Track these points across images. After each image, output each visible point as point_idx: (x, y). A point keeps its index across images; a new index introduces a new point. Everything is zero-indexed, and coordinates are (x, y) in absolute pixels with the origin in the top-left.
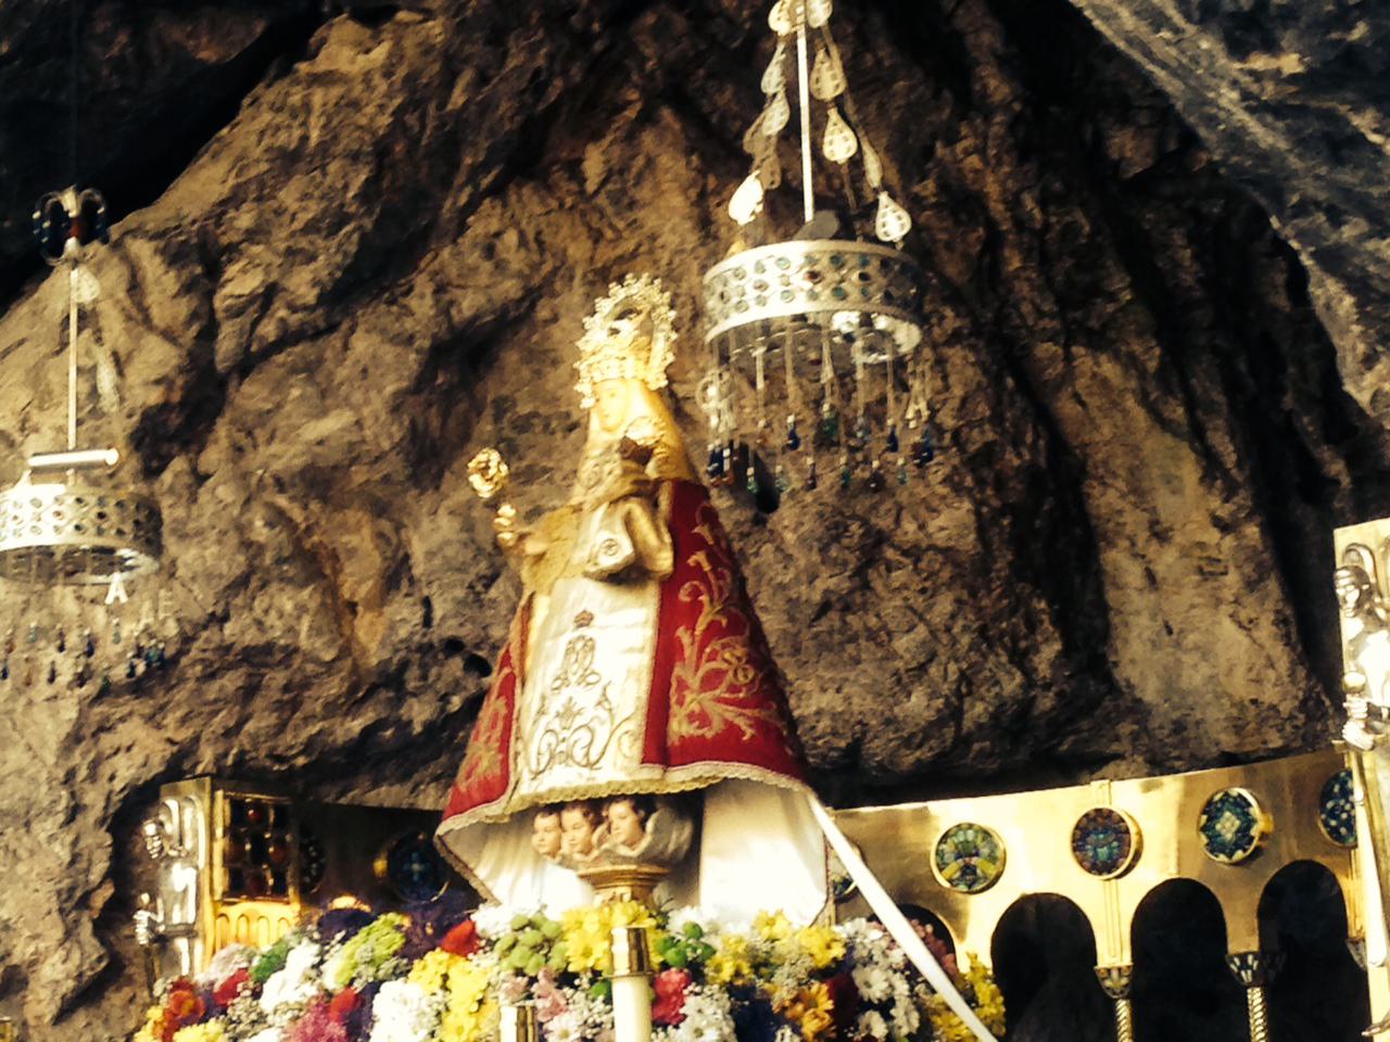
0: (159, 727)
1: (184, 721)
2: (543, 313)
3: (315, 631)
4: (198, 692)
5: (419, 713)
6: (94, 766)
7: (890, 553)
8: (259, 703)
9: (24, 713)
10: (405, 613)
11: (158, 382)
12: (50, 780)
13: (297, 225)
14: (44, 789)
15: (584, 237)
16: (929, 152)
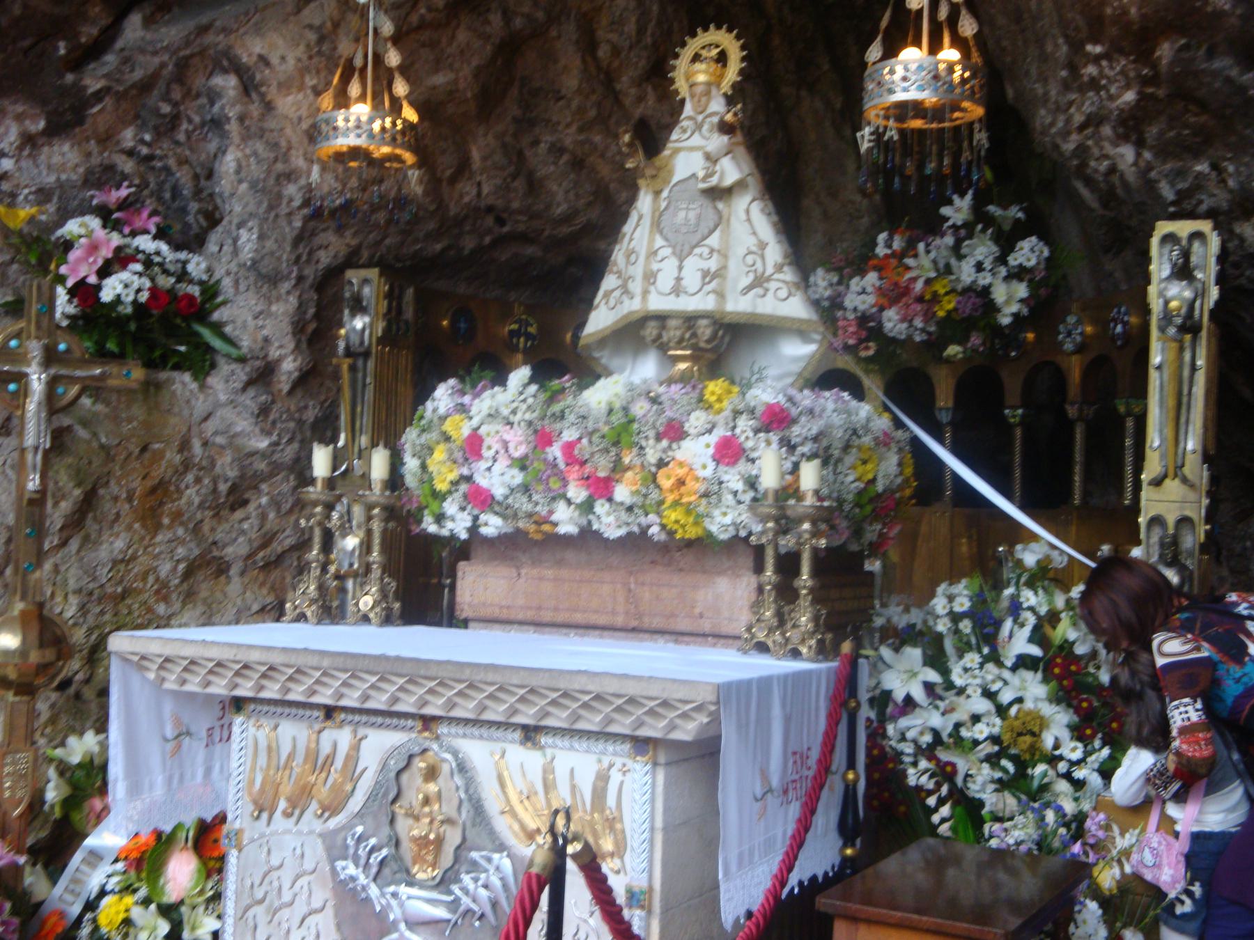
0: (342, 236)
2: (554, 33)
5: (469, 243)
6: (310, 254)
10: (468, 189)
12: (288, 261)
14: (284, 265)
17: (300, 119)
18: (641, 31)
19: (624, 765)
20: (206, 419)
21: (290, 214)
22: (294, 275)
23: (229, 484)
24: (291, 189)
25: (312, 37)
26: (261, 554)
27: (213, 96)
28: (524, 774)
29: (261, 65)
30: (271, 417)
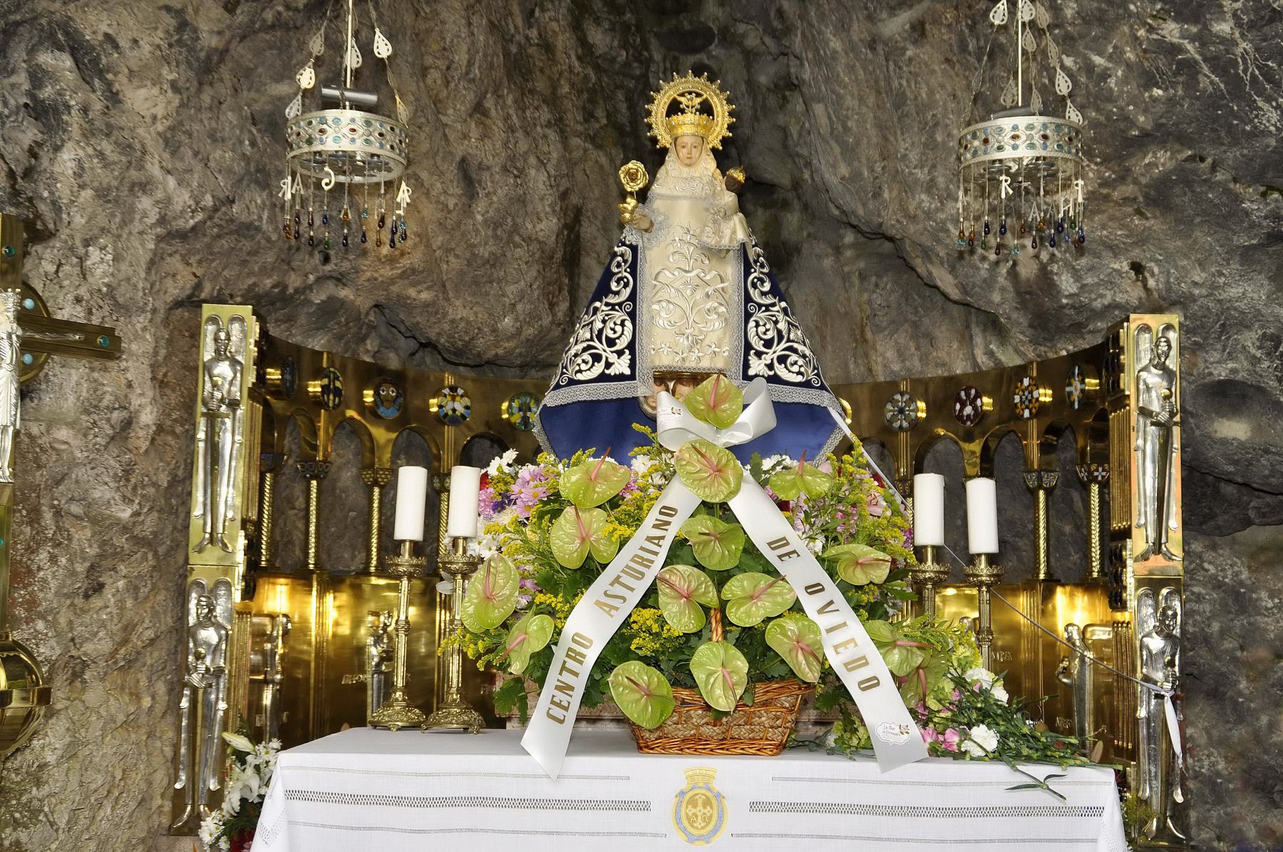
0: (188, 264)
1: (200, 262)
4: (209, 246)
5: (294, 281)
7: (517, 239)
9: (128, 239)
11: (220, 33)
12: (144, 289)
14: (141, 294)
15: (411, 11)
16: (532, 13)
17: (154, 118)
18: (470, 63)
20: (58, 483)
21: (141, 233)
23: (87, 564)
24: (145, 203)
25: (170, 21)
26: (122, 651)
27: (38, 77)
29: (108, 47)
30: (133, 480)
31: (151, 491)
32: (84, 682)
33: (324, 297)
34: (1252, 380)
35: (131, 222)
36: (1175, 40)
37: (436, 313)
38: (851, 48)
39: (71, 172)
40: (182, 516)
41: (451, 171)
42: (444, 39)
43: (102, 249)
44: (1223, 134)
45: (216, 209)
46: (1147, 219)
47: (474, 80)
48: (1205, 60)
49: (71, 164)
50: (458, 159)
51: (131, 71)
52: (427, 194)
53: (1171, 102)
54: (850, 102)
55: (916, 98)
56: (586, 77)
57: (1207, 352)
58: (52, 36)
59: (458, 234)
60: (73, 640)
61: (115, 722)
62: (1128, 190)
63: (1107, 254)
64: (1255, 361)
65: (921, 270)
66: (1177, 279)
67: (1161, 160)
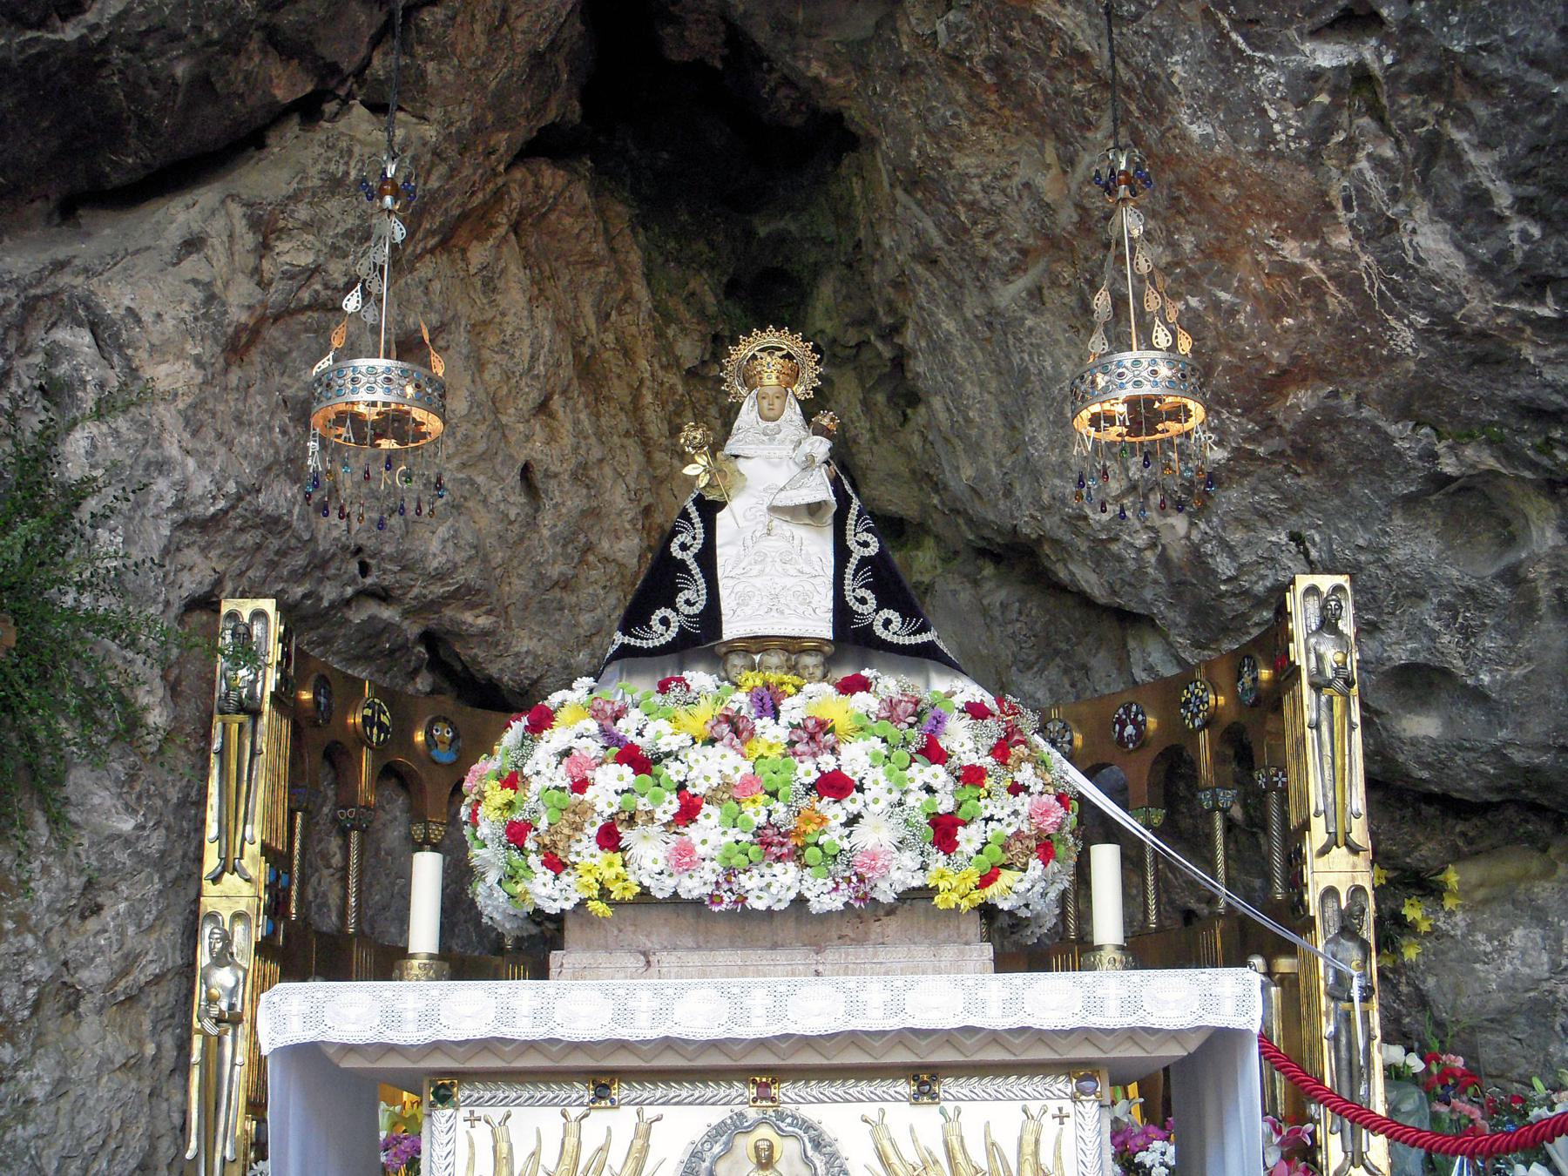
1: (221, 556)
3: (302, 517)
4: (231, 541)
5: (329, 593)
8: (259, 558)
11: (250, 307)
13: (339, 230)
16: (608, 315)
18: (533, 358)
19: (1060, 1110)
22: (162, 598)
24: (161, 485)
25: (198, 295)
26: (122, 984)
27: (53, 355)
28: (915, 1141)
29: (129, 320)
30: (138, 789)
31: (159, 803)
32: (78, 1016)
33: (364, 616)
34: (1434, 662)
35: (145, 504)
36: (1297, 261)
37: (497, 644)
38: (968, 327)
39: (82, 451)
40: (194, 844)
41: (513, 478)
42: (503, 331)
43: (112, 530)
44: (1361, 362)
45: (240, 498)
46: (1298, 475)
47: (538, 376)
48: (1330, 278)
49: (85, 443)
50: (520, 465)
51: (152, 346)
52: (485, 501)
53: (1303, 330)
54: (969, 389)
55: (1040, 373)
56: (672, 388)
57: (1382, 631)
58: (73, 310)
59: (521, 549)
60: (65, 964)
61: (112, 1063)
62: (1276, 443)
63: (1262, 525)
64: (1433, 635)
65: (1063, 574)
66: (1340, 545)
67: (1303, 399)
